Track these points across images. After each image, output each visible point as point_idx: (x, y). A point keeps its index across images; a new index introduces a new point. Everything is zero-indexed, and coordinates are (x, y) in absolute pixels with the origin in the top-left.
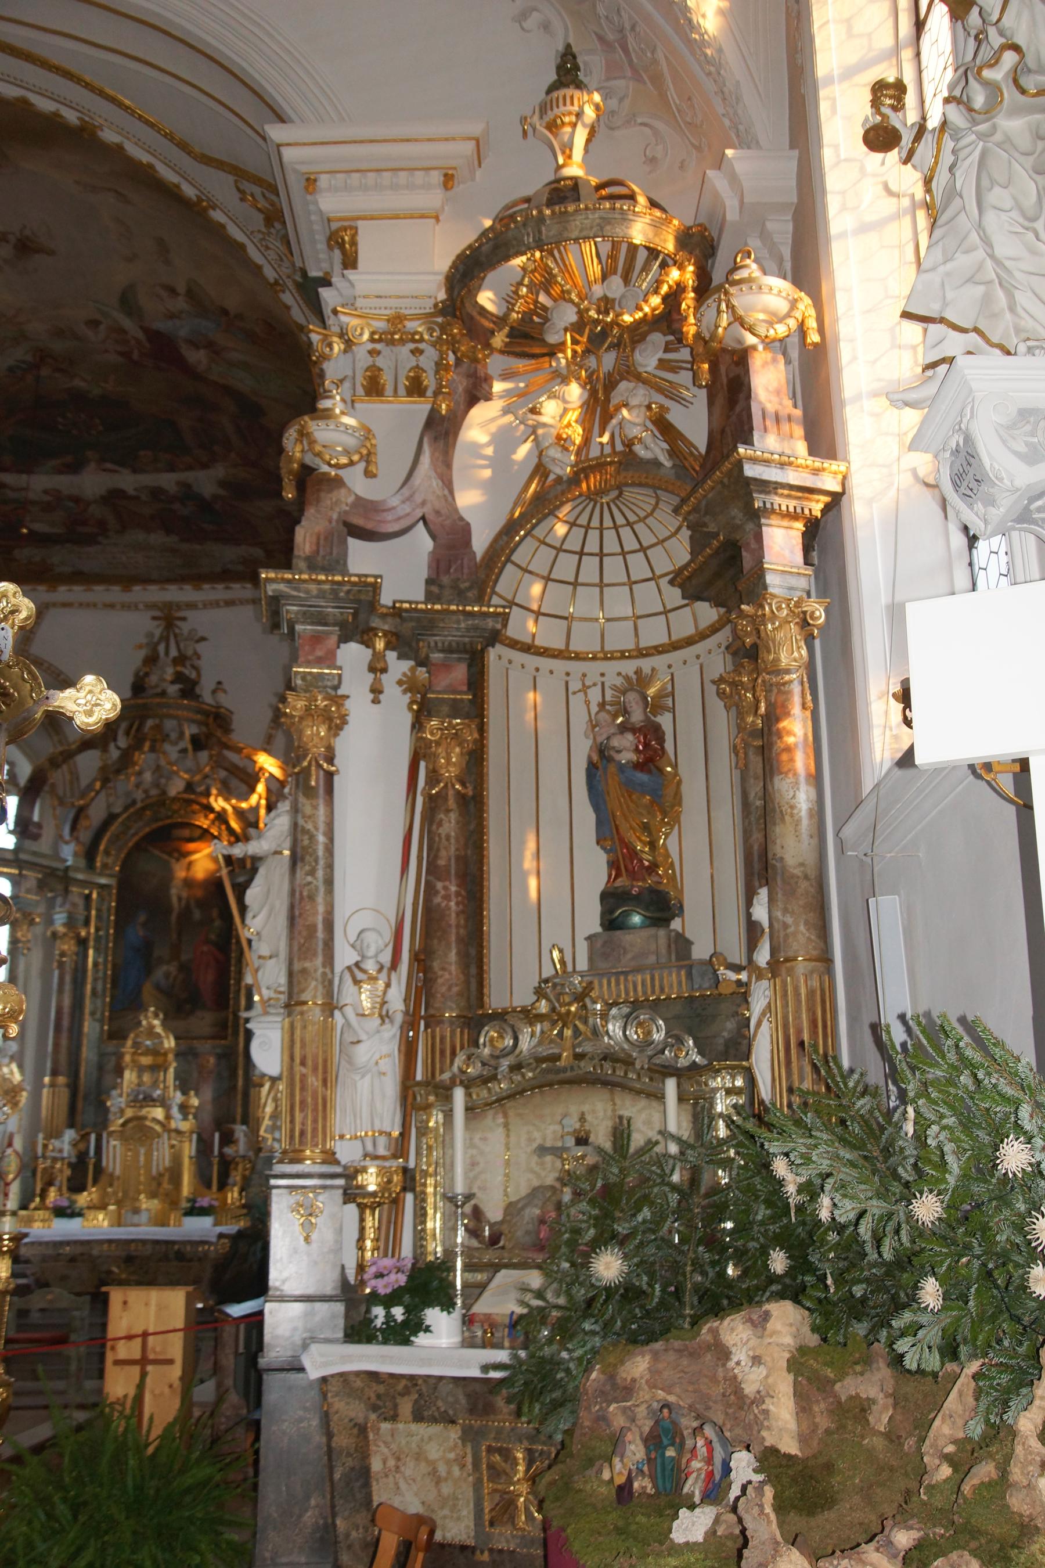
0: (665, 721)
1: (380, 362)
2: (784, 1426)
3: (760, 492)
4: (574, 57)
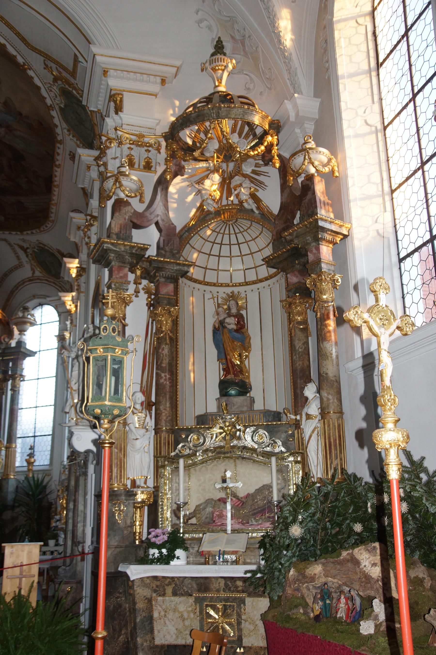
0: (243, 312)
1: (133, 153)
3: (321, 232)
4: (222, 42)
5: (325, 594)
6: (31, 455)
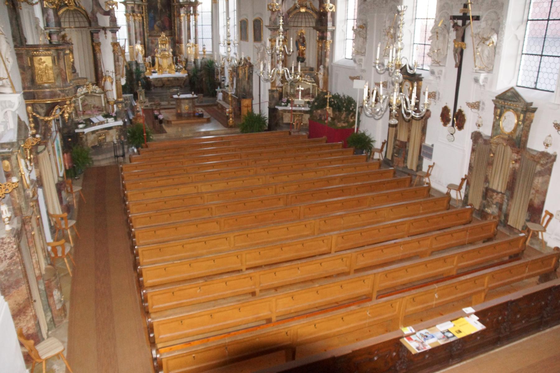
2: (332, 116)
5: (320, 115)
6: (204, 48)
